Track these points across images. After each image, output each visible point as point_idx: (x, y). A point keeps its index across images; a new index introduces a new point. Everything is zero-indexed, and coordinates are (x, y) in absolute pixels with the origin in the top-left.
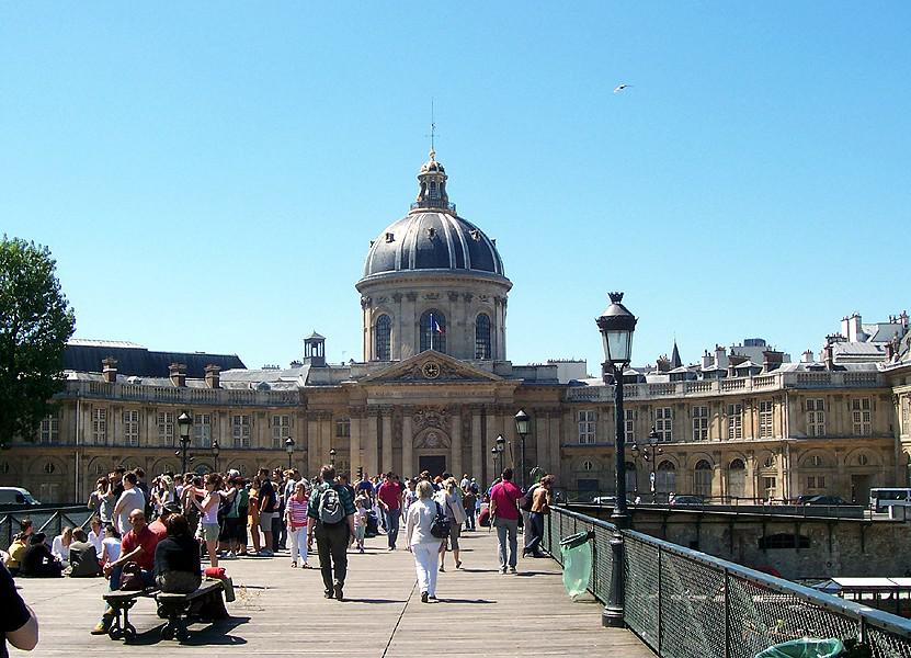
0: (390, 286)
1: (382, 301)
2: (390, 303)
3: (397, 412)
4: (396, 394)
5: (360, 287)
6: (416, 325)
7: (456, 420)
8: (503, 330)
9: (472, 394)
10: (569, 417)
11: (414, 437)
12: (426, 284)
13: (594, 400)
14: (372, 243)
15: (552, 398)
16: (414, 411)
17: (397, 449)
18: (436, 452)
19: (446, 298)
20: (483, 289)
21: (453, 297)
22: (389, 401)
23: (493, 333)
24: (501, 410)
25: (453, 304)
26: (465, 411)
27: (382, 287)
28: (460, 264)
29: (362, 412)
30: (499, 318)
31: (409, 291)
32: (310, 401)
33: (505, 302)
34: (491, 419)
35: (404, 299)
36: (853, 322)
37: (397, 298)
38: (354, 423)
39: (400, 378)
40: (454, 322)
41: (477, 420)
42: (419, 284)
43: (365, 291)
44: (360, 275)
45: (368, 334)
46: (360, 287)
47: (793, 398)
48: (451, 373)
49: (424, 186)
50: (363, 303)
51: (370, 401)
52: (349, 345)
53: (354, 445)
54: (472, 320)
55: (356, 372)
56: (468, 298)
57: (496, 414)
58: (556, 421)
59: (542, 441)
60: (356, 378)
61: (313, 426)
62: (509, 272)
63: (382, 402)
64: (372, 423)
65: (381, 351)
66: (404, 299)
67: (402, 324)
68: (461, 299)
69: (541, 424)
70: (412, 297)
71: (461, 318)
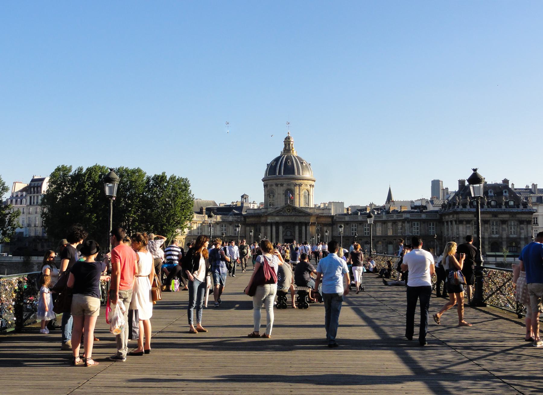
0: (275, 181)
1: (272, 185)
2: (274, 187)
3: (277, 224)
4: (277, 219)
5: (263, 180)
7: (297, 228)
9: (302, 219)
10: (334, 226)
12: (287, 180)
16: (284, 224)
20: (306, 182)
26: (300, 224)
27: (271, 181)
28: (299, 173)
29: (266, 224)
32: (247, 220)
38: (262, 228)
39: (278, 213)
41: (304, 228)
42: (284, 180)
43: (266, 182)
46: (263, 180)
47: (408, 222)
49: (285, 145)
51: (269, 221)
52: (256, 198)
56: (300, 185)
58: (330, 228)
61: (248, 228)
67: (278, 194)
70: (282, 185)
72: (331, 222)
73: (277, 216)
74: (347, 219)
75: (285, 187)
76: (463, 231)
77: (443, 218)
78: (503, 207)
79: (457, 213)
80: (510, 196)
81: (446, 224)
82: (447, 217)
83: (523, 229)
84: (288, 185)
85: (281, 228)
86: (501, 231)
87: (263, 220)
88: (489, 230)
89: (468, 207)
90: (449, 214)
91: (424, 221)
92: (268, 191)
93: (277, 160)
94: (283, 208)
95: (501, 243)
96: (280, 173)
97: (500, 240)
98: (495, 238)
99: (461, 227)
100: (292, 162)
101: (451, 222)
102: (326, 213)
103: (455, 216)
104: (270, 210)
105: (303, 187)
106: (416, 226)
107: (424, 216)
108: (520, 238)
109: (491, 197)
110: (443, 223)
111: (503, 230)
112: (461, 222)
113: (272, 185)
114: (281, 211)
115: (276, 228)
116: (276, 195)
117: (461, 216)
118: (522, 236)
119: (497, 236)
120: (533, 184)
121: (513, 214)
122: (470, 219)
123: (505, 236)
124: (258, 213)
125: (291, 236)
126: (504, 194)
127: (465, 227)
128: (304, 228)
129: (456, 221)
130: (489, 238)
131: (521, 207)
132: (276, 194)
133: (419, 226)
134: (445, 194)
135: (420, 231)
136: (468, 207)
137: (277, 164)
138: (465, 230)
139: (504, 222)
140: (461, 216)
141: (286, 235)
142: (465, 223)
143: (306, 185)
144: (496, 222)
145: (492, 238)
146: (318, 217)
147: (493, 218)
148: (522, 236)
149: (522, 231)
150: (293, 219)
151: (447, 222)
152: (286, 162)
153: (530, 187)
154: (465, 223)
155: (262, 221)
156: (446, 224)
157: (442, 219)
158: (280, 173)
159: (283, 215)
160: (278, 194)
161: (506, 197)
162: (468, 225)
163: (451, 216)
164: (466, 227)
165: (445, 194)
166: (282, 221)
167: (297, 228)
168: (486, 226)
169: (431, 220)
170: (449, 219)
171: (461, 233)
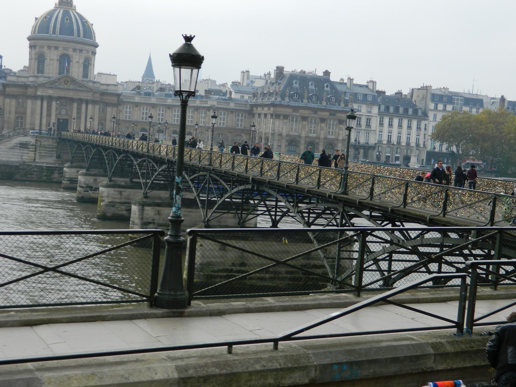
1: (42, 47)
3: (50, 98)
5: (29, 39)
6: (57, 60)
7: (75, 105)
8: (94, 65)
9: (83, 96)
10: (120, 108)
11: (56, 109)
12: (63, 43)
13: (132, 101)
14: (36, 19)
15: (115, 99)
16: (59, 98)
17: (49, 115)
18: (65, 117)
19: (71, 50)
20: (87, 47)
21: (75, 50)
22: (47, 94)
23: (90, 67)
24: (94, 102)
25: (74, 53)
26: (80, 101)
27: (42, 41)
28: (79, 35)
29: (35, 97)
30: (93, 60)
31: (55, 45)
32: (7, 89)
33: (94, 53)
34: (90, 107)
35: (53, 48)
36: (246, 74)
37: (49, 47)
39: (52, 84)
40: (74, 61)
41: (84, 106)
42: (60, 43)
43: (33, 42)
44: (29, 34)
45: (33, 61)
46: (29, 39)
48: (75, 84)
50: (31, 47)
53: (29, 111)
54: (82, 61)
55: (31, 79)
56: (81, 51)
57: (92, 104)
58: (115, 109)
59: (109, 117)
60: (32, 82)
61: (8, 100)
62: (98, 41)
63: (44, 94)
64: (39, 103)
65: (40, 70)
66: (53, 48)
68: (78, 51)
69: (109, 109)
70: (56, 48)
71: (77, 59)
72: (116, 102)
73: (51, 88)
74: (137, 99)
75: (60, 51)
76: (279, 128)
77: (255, 109)
78: (324, 103)
79: (273, 105)
80: (331, 91)
81: (257, 116)
82: (260, 109)
83: (342, 130)
84: (65, 49)
85: (54, 104)
86: (319, 130)
87: (30, 91)
88: (307, 128)
89: (287, 99)
90: (263, 106)
91: (232, 111)
92: (36, 54)
93: (50, 14)
94: (59, 79)
95: (318, 144)
96: (54, 32)
97: (317, 140)
98: (312, 137)
99: (277, 122)
100: (71, 19)
101: (266, 115)
102: (111, 89)
103: (272, 109)
104: (41, 80)
105: (84, 54)
106: (222, 116)
107: (232, 105)
108: (337, 140)
109: (312, 90)
110: (253, 115)
111: (322, 129)
112: (278, 116)
113: (42, 47)
114: (55, 82)
115: (48, 103)
116: (47, 62)
117: (279, 110)
118: (340, 138)
119: (315, 135)
120: (349, 78)
121: (333, 113)
122: (288, 114)
123: (322, 136)
124: (22, 82)
125: (66, 115)
126: (326, 88)
127: (281, 122)
128: (84, 106)
129: (272, 115)
130: (306, 137)
131: (342, 105)
132: (48, 58)
133: (225, 117)
134: (245, 78)
135: (227, 122)
136: (287, 99)
137: (50, 19)
138: (281, 126)
139: (323, 120)
140: (279, 110)
141: (60, 113)
142: (281, 118)
143: (88, 51)
144: (315, 120)
145: (309, 137)
146: (103, 94)
147: (312, 115)
148: (340, 138)
149: (341, 132)
150: (71, 94)
151: (259, 115)
152: (63, 18)
153: (345, 81)
154: (281, 118)
155: (29, 93)
156: (257, 116)
157: (252, 110)
158: (54, 32)
159: (58, 88)
160: (51, 59)
161: (327, 91)
162: (285, 121)
163: (266, 109)
164: (283, 123)
165: (245, 78)
166: (56, 95)
167: (75, 105)
168: (304, 123)
169: (238, 110)
170: (263, 112)
171: (276, 128)
